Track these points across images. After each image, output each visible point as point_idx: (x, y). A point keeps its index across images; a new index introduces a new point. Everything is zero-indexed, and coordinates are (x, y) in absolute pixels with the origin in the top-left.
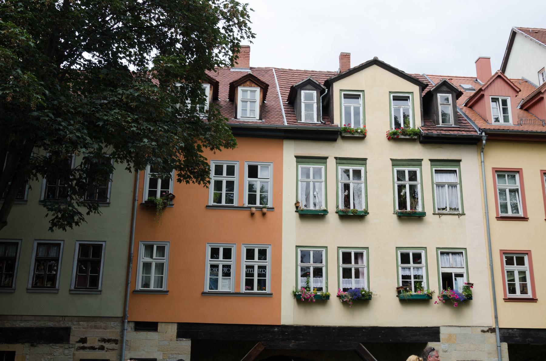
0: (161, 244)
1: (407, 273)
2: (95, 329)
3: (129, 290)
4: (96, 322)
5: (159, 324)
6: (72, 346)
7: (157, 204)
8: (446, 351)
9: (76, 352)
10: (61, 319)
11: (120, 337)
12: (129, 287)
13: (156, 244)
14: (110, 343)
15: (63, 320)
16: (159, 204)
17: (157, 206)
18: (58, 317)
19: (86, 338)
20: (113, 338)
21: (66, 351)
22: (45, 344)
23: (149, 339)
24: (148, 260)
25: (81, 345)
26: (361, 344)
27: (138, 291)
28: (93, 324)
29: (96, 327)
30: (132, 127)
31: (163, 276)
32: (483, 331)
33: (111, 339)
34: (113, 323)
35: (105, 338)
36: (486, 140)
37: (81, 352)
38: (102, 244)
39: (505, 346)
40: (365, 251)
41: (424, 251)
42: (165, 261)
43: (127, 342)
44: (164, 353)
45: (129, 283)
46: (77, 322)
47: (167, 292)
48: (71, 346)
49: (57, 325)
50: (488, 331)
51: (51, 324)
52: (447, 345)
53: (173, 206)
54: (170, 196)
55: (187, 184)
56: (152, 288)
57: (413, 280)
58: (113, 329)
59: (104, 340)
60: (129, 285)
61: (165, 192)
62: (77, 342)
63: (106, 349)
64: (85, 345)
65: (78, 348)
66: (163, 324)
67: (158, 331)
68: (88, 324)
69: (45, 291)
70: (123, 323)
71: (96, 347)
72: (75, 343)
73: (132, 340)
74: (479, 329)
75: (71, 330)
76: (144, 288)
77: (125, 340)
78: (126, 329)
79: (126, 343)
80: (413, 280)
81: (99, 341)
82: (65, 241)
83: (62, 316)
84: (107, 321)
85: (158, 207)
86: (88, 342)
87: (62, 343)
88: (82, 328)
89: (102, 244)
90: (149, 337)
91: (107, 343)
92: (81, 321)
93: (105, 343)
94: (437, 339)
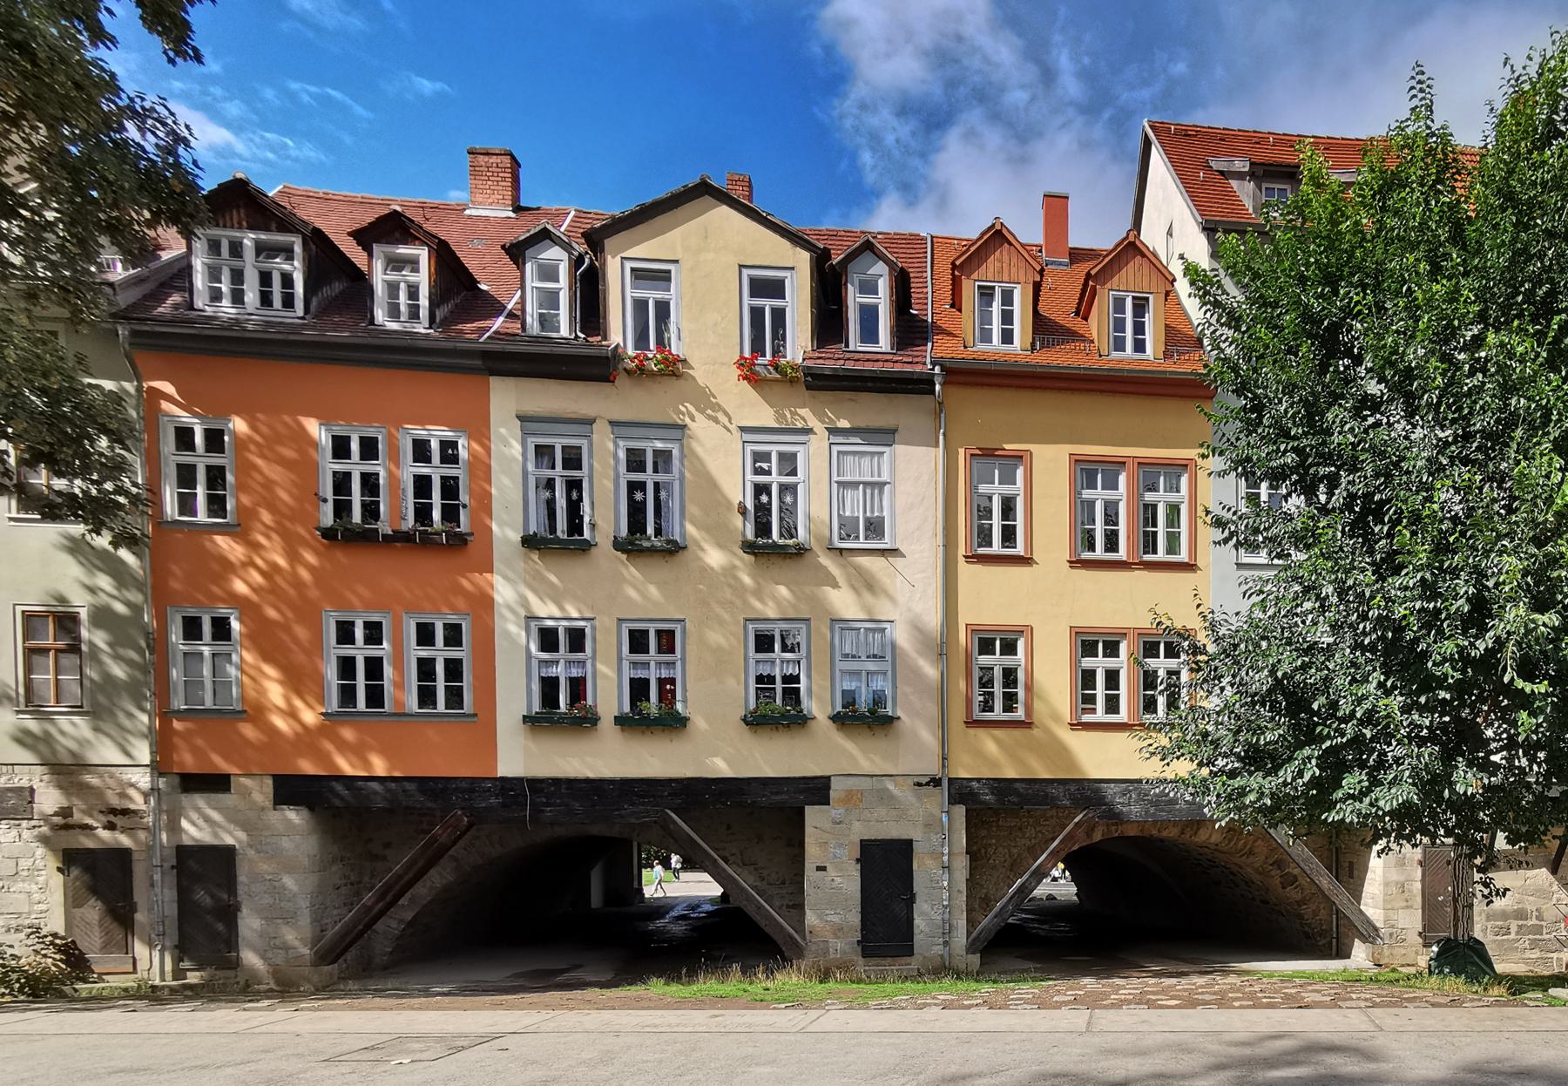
1: (765, 670)
8: (840, 823)
26: (669, 812)
32: (919, 784)
36: (942, 385)
39: (960, 811)
40: (679, 626)
41: (804, 626)
50: (928, 784)
52: (841, 811)
57: (779, 686)
74: (910, 781)
80: (779, 686)
94: (824, 800)
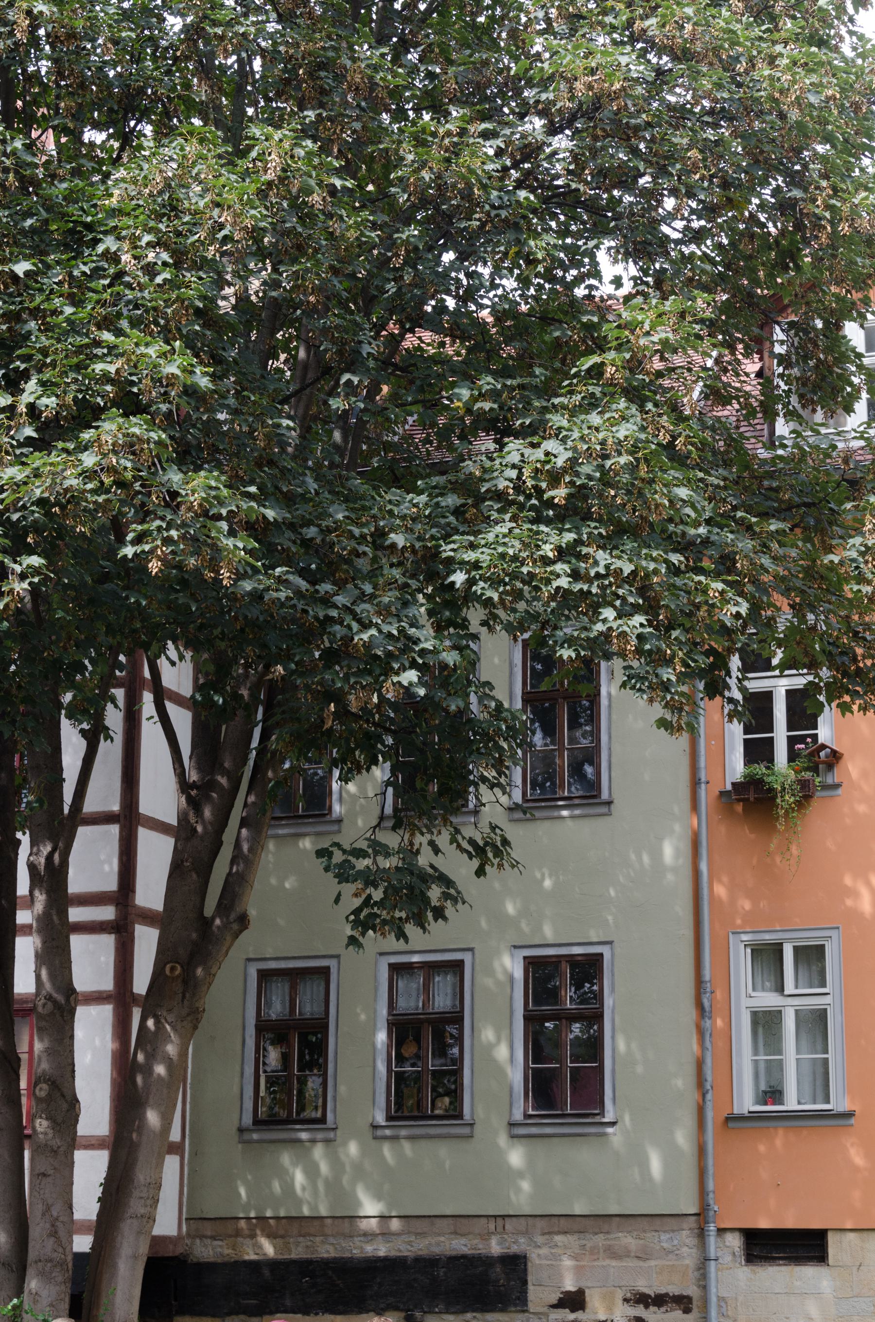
0: (810, 939)
2: (612, 1258)
3: (710, 1114)
4: (608, 1233)
7: (771, 790)
10: (492, 1227)
11: (699, 1286)
12: (709, 1106)
13: (789, 940)
14: (663, 1309)
15: (500, 1229)
16: (784, 789)
17: (774, 798)
18: (483, 1221)
20: (674, 1290)
22: (447, 1313)
23: (801, 1294)
24: (768, 1000)
27: (741, 1118)
28: (599, 1240)
30: (558, 576)
31: (829, 1056)
33: (667, 1295)
34: (668, 1236)
35: (647, 1291)
38: (601, 955)
42: (827, 1000)
43: (723, 1304)
45: (707, 1091)
46: (547, 1237)
47: (849, 1115)
49: (481, 1246)
51: (460, 1246)
53: (840, 791)
54: (822, 754)
55: (843, 715)
56: (791, 1103)
58: (671, 1256)
60: (709, 1096)
61: (802, 739)
62: (554, 1306)
68: (583, 1242)
69: (432, 1131)
70: (702, 1234)
72: (545, 1309)
73: (741, 1298)
75: (529, 1264)
76: (765, 1103)
77: (714, 1299)
78: (712, 1255)
79: (720, 1306)
81: (626, 1300)
82: (476, 951)
83: (495, 1217)
84: (645, 1231)
85: (779, 800)
87: (503, 1310)
89: (601, 955)
91: (655, 1309)
92: (559, 1233)
93: (647, 1307)
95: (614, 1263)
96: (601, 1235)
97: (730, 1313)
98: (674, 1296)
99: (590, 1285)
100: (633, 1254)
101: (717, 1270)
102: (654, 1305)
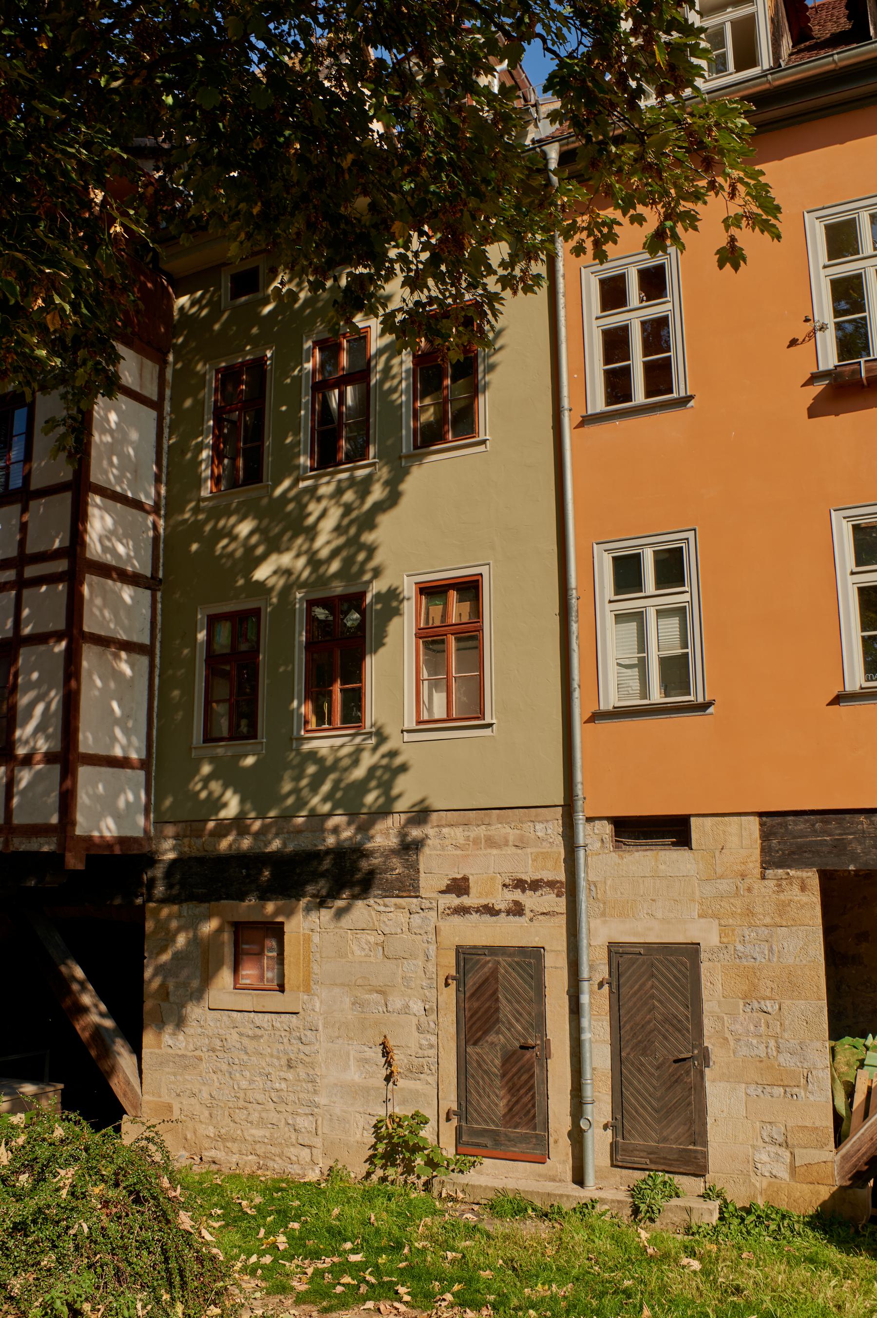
2: (492, 847)
4: (489, 825)
5: (693, 820)
6: (428, 905)
9: (441, 924)
14: (538, 893)
19: (465, 879)
21: (416, 920)
23: (665, 877)
25: (453, 900)
28: (482, 831)
29: (491, 843)
33: (541, 880)
37: (456, 919)
44: (723, 923)
48: (426, 904)
58: (544, 844)
59: (520, 884)
62: (442, 892)
63: (527, 911)
64: (466, 901)
65: (448, 911)
66: (709, 821)
67: (694, 845)
71: (497, 907)
72: (435, 895)
73: (609, 882)
86: (473, 891)
88: (450, 848)
90: (662, 867)
93: (523, 891)
95: (495, 851)
96: (483, 827)
97: (599, 896)
98: (548, 881)
99: (473, 872)
100: (511, 843)
101: (586, 856)
102: (530, 890)
